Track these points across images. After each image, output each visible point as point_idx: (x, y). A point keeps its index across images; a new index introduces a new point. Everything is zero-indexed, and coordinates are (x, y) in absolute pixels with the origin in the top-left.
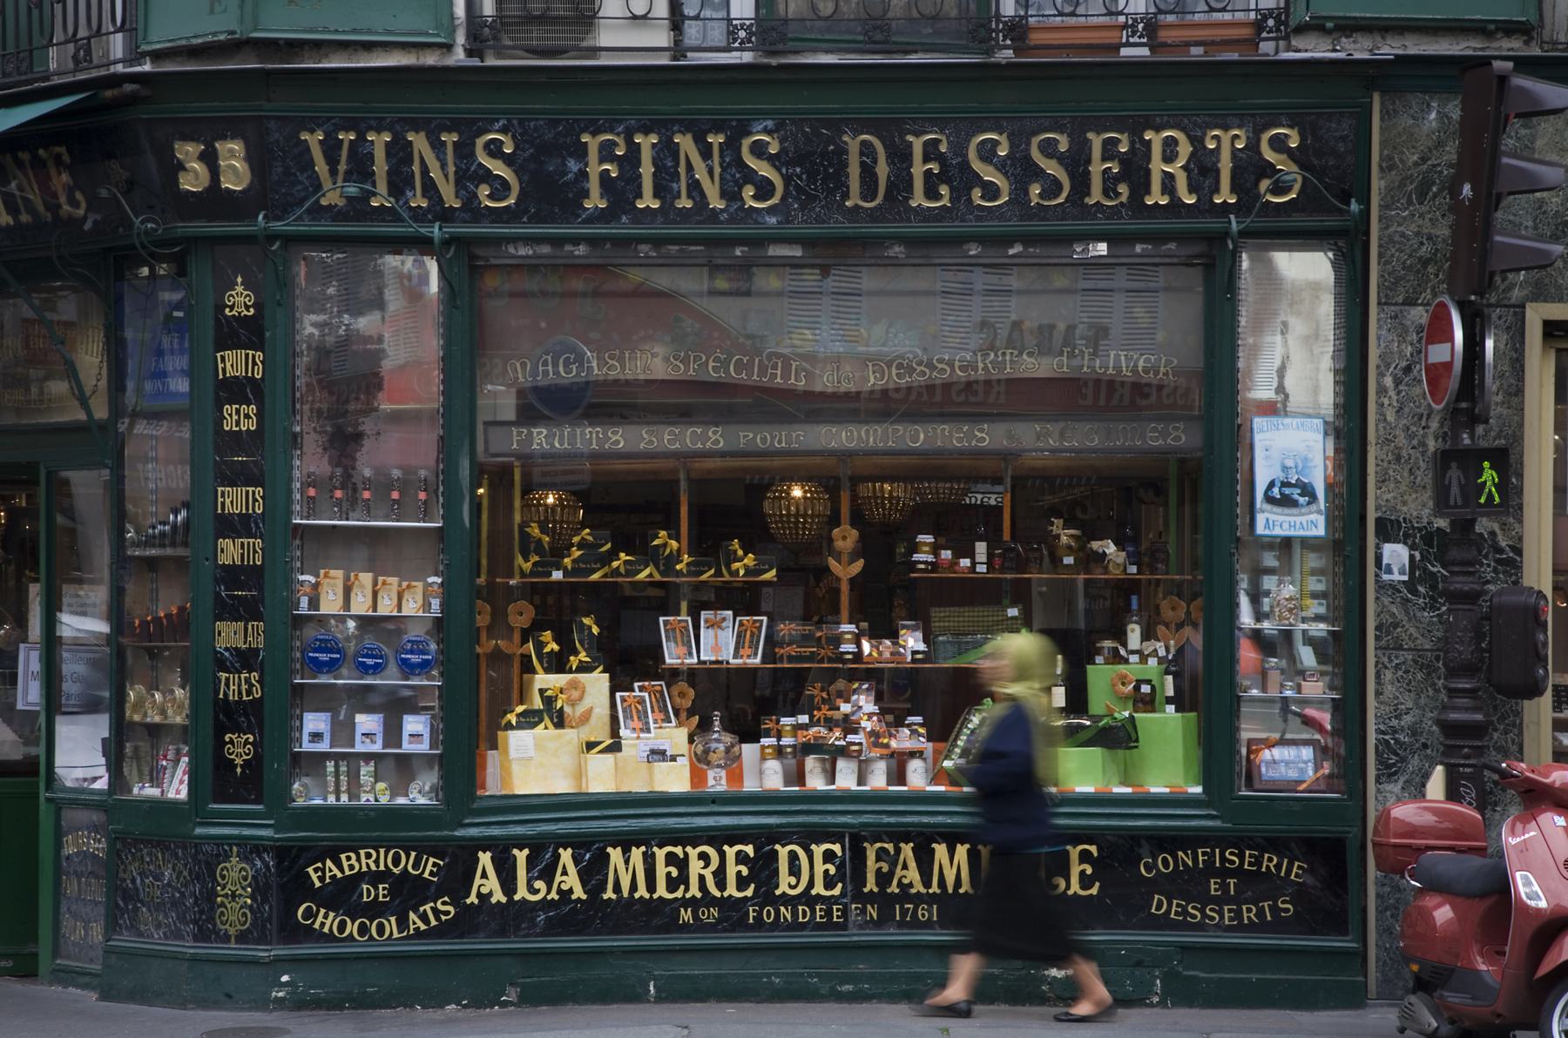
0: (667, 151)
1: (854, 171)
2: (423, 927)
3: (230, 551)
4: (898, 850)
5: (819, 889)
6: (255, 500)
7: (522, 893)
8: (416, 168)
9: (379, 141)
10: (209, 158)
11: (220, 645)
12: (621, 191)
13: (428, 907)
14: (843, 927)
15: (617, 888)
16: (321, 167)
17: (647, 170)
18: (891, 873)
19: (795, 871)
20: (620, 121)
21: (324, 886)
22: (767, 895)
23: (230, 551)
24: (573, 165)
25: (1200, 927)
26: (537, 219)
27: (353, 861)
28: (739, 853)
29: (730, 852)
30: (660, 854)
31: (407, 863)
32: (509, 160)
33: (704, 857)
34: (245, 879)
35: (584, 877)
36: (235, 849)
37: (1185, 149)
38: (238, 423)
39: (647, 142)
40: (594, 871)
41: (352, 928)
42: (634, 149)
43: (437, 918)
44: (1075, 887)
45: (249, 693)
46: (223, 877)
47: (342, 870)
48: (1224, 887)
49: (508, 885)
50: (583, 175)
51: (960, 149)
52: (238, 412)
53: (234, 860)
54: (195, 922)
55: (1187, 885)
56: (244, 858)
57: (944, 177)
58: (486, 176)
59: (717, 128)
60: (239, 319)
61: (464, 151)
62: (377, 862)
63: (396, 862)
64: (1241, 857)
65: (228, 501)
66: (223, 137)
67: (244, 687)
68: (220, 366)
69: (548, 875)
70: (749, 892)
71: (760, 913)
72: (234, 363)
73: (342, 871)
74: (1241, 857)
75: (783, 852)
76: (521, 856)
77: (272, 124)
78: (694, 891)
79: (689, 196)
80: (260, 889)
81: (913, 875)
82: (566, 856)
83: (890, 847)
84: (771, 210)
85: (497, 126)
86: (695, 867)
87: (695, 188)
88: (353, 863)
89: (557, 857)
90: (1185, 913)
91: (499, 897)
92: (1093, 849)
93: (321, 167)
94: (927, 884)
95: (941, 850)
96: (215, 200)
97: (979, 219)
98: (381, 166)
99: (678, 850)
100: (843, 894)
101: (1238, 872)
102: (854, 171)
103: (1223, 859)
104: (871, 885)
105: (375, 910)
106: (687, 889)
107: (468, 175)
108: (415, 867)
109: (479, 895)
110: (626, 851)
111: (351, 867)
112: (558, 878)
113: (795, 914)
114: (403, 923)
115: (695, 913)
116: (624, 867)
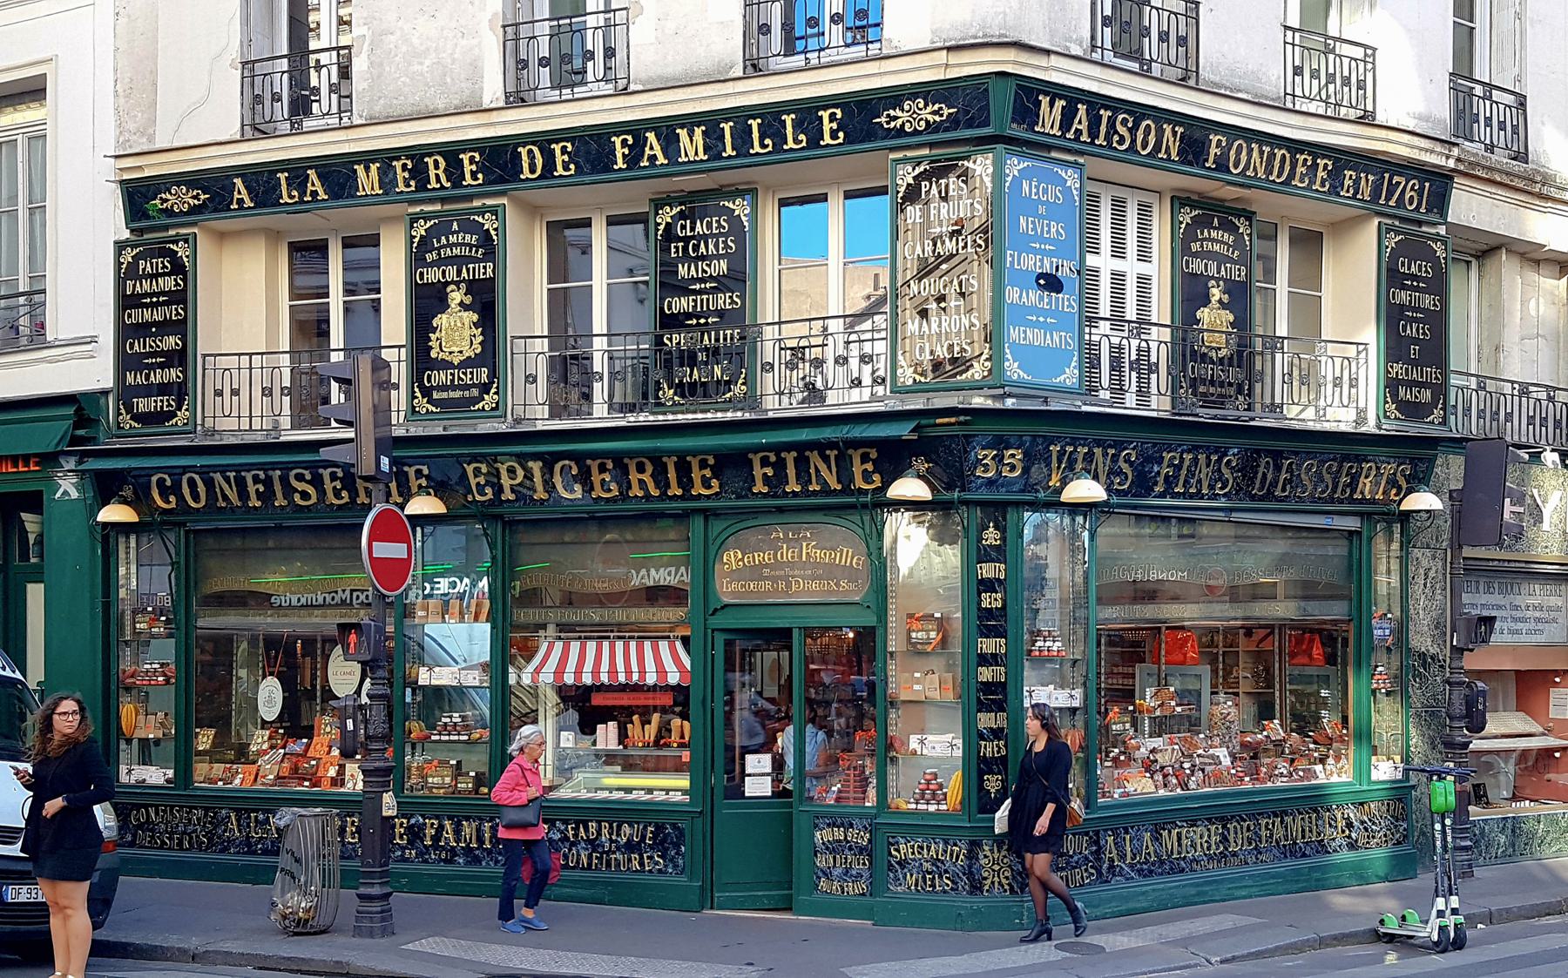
0: (1195, 461)
1: (1260, 475)
3: (986, 674)
6: (1000, 646)
8: (1093, 467)
11: (981, 726)
16: (1054, 464)
17: (1184, 472)
20: (1180, 445)
23: (986, 674)
24: (1156, 469)
32: (1131, 464)
37: (1373, 473)
38: (990, 603)
39: (1188, 457)
42: (1182, 460)
50: (1158, 473)
51: (1299, 466)
52: (990, 597)
57: (1290, 481)
58: (1120, 473)
60: (990, 546)
61: (1115, 458)
65: (984, 646)
67: (996, 749)
72: (987, 571)
84: (1224, 495)
85: (1132, 446)
87: (1199, 481)
93: (1054, 464)
102: (1260, 475)
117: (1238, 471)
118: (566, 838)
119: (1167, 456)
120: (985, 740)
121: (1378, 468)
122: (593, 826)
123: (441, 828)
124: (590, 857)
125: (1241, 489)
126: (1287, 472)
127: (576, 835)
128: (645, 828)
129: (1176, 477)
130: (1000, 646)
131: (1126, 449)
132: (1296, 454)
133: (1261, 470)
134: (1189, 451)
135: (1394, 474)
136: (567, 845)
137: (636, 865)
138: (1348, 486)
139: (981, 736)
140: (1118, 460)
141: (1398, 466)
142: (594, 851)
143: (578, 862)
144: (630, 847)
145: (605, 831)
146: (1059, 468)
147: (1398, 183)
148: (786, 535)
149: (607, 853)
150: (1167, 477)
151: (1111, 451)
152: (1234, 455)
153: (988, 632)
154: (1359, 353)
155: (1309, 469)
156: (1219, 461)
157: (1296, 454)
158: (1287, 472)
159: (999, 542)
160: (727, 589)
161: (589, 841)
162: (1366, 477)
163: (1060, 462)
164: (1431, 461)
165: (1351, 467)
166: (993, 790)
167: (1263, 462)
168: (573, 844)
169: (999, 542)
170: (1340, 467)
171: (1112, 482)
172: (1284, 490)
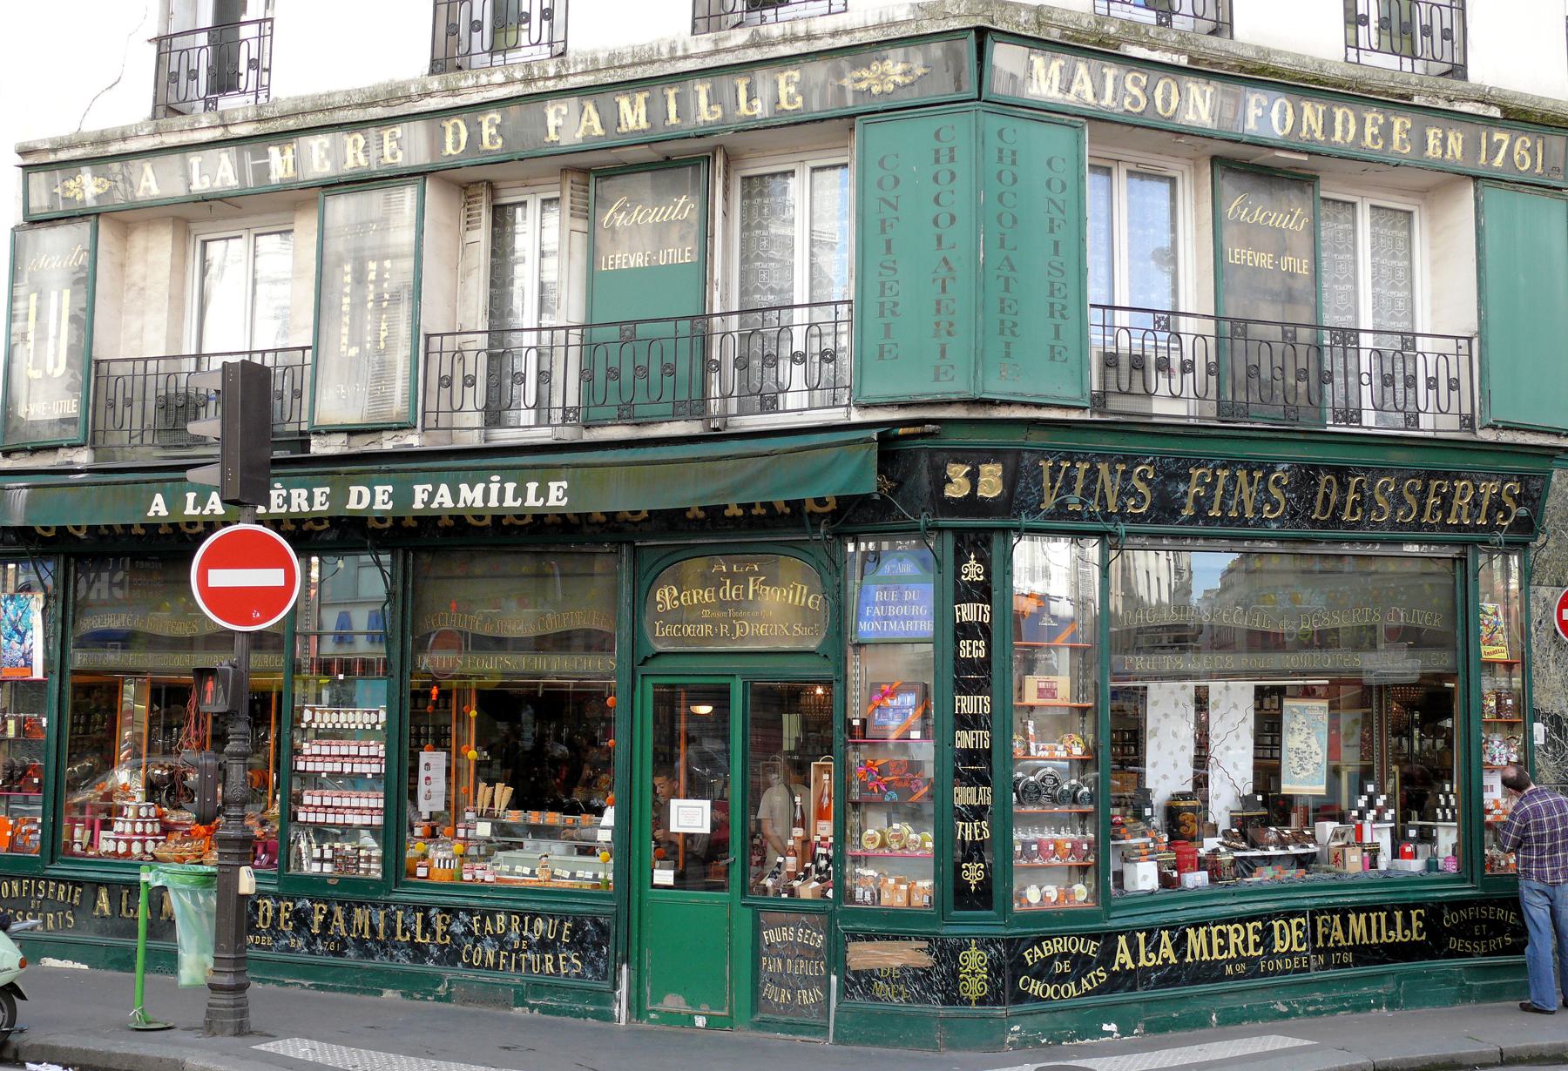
0: (1233, 478)
1: (1320, 497)
3: (965, 739)
4: (1332, 919)
5: (1295, 948)
6: (984, 705)
7: (1143, 962)
8: (1098, 486)
9: (1083, 467)
10: (973, 477)
11: (958, 803)
13: (1091, 975)
14: (1307, 970)
15: (1193, 955)
16: (1047, 484)
17: (1219, 492)
18: (1330, 934)
19: (1283, 938)
20: (1211, 461)
21: (1034, 964)
22: (1269, 954)
23: (965, 739)
24: (1182, 488)
25: (1470, 955)
26: (1156, 521)
29: (1250, 926)
30: (1214, 930)
31: (1079, 946)
32: (1149, 483)
33: (1237, 931)
34: (982, 961)
35: (1176, 947)
36: (973, 941)
37: (1471, 492)
38: (971, 653)
39: (1223, 474)
40: (1180, 944)
42: (1215, 477)
44: (1415, 937)
46: (965, 961)
48: (1481, 930)
49: (1135, 957)
50: (1186, 493)
51: (1372, 486)
52: (971, 645)
53: (973, 949)
54: (943, 992)
56: (980, 947)
57: (1361, 503)
58: (1134, 493)
59: (1260, 467)
60: (972, 583)
61: (1127, 475)
64: (1488, 911)
65: (963, 705)
66: (988, 462)
67: (977, 831)
68: (958, 614)
69: (1156, 949)
70: (1260, 952)
72: (968, 612)
74: (1488, 911)
75: (1276, 925)
76: (1141, 937)
77: (1026, 455)
78: (1233, 954)
80: (995, 968)
81: (1339, 934)
82: (1165, 934)
83: (1328, 918)
84: (1275, 520)
85: (1148, 461)
86: (1233, 937)
87: (1241, 503)
88: (1050, 948)
89: (1160, 936)
90: (1464, 947)
91: (1130, 965)
92: (1422, 911)
93: (1047, 484)
94: (1347, 941)
95: (1352, 917)
96: (972, 504)
97: (1372, 528)
99: (1223, 928)
100: (1307, 950)
101: (1487, 921)
102: (1320, 497)
103: (1480, 913)
104: (1320, 944)
105: (1062, 978)
108: (1084, 948)
109: (1120, 964)
110: (1197, 930)
111: (1049, 950)
112: (1162, 950)
114: (1078, 985)
115: (1234, 968)
116: (1196, 940)
117: (1290, 492)
118: (470, 933)
119: (1196, 473)
120: (962, 820)
121: (1476, 488)
122: (500, 918)
123: (330, 914)
124: (497, 955)
125: (1297, 513)
126: (1355, 492)
127: (481, 929)
128: (561, 923)
129: (1210, 498)
130: (984, 705)
131: (1141, 464)
132: (1366, 470)
133: (1321, 490)
134: (1224, 467)
135: (1499, 494)
136: (471, 940)
137: (549, 967)
138: (1438, 508)
142: (502, 948)
143: (483, 961)
144: (544, 945)
145: (515, 926)
146: (1052, 487)
147: (1501, 142)
148: (730, 568)
149: (517, 951)
150: (1197, 498)
151: (1121, 467)
152: (1284, 471)
153: (964, 688)
154: (1459, 347)
155: (1384, 489)
156: (1265, 478)
157: (1366, 470)
158: (1355, 492)
159: (982, 578)
160: (661, 636)
161: (495, 936)
162: (1462, 498)
163: (1053, 480)
165: (1440, 486)
168: (478, 940)
169: (982, 578)
170: (1426, 487)
171: (1125, 505)
172: (1353, 513)
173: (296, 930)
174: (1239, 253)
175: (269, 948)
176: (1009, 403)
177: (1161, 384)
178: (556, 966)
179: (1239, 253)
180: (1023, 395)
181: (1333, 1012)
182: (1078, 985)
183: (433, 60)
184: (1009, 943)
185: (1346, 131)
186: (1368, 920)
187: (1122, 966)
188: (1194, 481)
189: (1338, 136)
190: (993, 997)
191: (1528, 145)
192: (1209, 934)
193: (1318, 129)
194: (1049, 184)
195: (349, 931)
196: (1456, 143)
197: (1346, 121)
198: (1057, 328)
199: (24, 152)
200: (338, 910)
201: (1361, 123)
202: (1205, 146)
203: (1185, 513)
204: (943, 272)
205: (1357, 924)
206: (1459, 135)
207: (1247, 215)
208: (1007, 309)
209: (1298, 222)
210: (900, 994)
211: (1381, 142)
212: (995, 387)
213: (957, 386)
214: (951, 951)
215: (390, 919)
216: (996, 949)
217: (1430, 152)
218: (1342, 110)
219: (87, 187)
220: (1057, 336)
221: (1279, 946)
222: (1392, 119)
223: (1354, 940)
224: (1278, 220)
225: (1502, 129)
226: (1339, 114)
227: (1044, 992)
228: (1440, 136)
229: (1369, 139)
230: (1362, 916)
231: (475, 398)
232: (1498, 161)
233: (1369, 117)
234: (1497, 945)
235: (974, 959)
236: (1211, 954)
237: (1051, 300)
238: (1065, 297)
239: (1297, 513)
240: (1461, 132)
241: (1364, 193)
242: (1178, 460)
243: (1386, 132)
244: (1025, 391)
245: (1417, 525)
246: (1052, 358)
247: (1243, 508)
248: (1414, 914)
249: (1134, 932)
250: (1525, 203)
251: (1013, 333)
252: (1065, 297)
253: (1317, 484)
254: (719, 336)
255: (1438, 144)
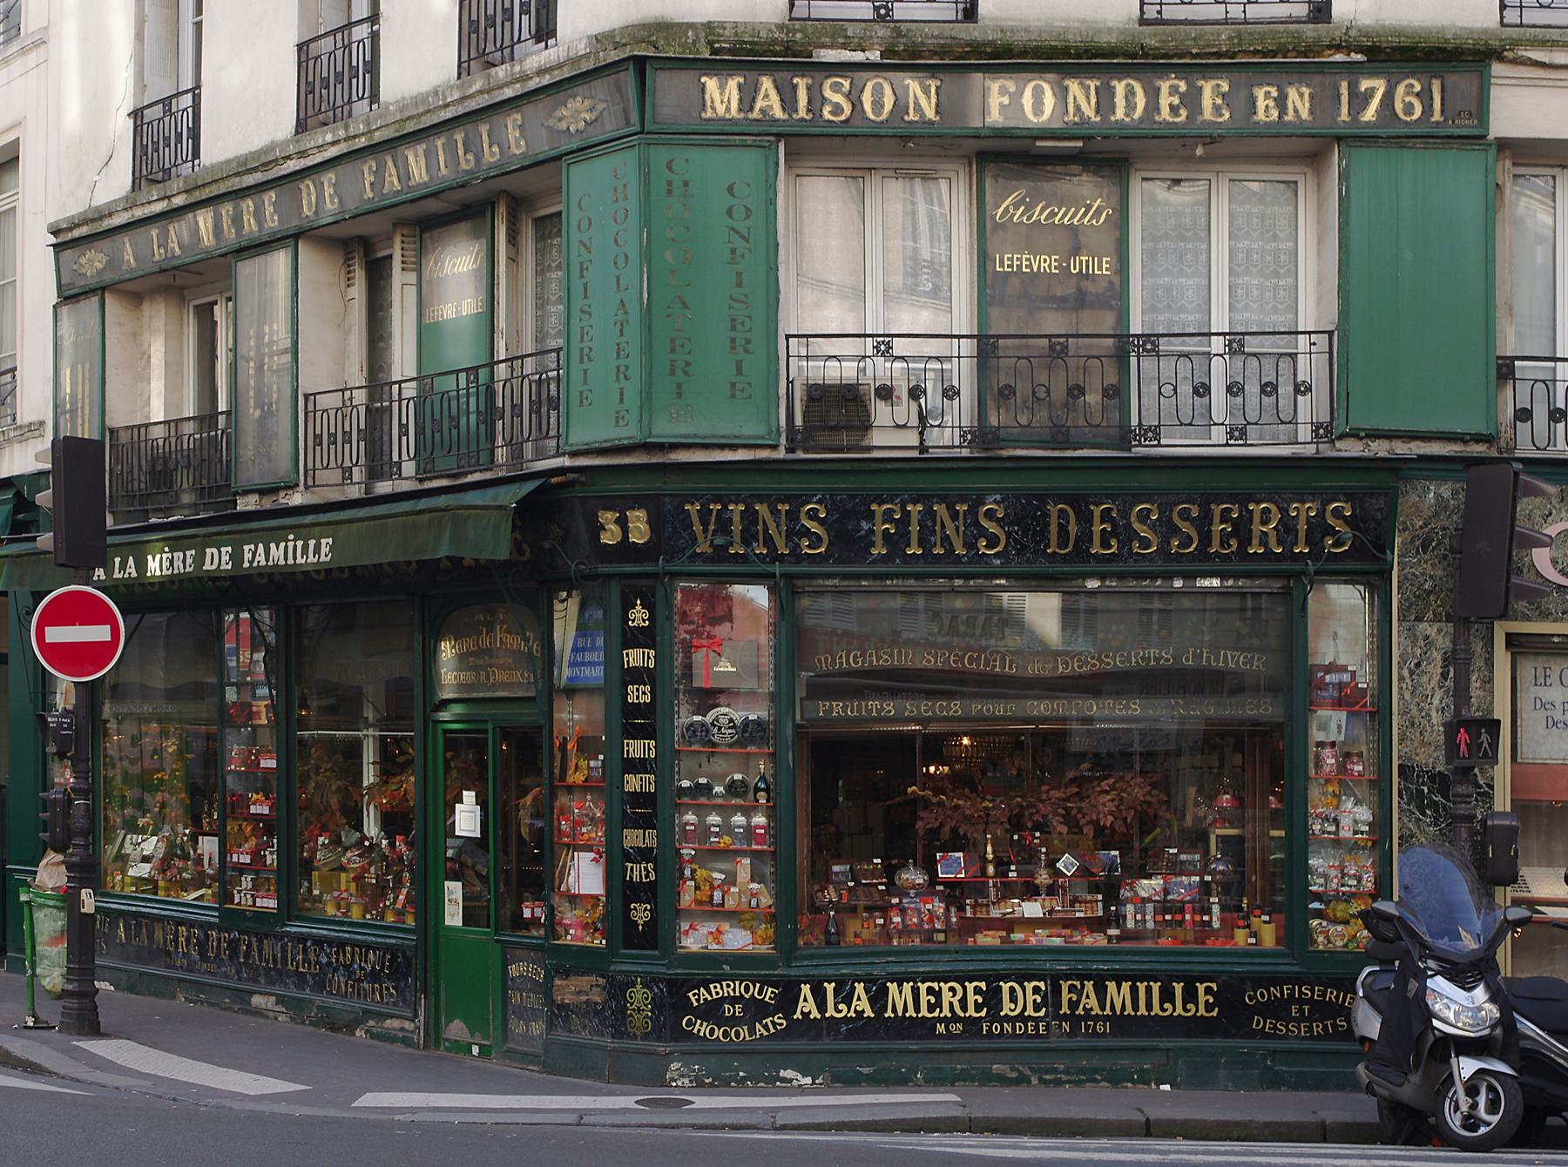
0: (929, 514)
1: (1054, 528)
2: (766, 1033)
3: (633, 783)
4: (1083, 986)
5: (1030, 1012)
7: (830, 1012)
12: (895, 542)
13: (768, 1020)
15: (894, 1010)
17: (914, 528)
18: (1079, 1001)
19: (1013, 999)
20: (897, 496)
21: (700, 1005)
22: (994, 1016)
23: (633, 783)
24: (865, 525)
25: (1285, 1037)
26: (839, 561)
27: (718, 989)
28: (976, 987)
29: (970, 987)
30: (923, 987)
31: (754, 991)
32: (822, 522)
33: (952, 989)
35: (872, 1001)
38: (638, 698)
39: (915, 509)
40: (878, 998)
41: (719, 1033)
42: (906, 515)
43: (775, 1028)
44: (1202, 1011)
45: (647, 877)
47: (711, 995)
48: (1301, 1011)
50: (871, 531)
51: (1125, 514)
53: (639, 986)
54: (613, 1026)
55: (1276, 1009)
56: (645, 985)
57: (1114, 533)
58: (806, 532)
59: (963, 500)
61: (793, 516)
62: (734, 990)
63: (747, 989)
67: (644, 873)
70: (983, 1014)
71: (991, 1027)
72: (635, 657)
73: (711, 995)
75: (1005, 987)
76: (830, 988)
78: (946, 1012)
79: (942, 545)
80: (657, 1005)
81: (1093, 1002)
82: (860, 987)
83: (1078, 984)
85: (815, 499)
86: (947, 996)
87: (946, 540)
88: (718, 990)
90: (1275, 1028)
91: (815, 1014)
94: (1103, 1009)
95: (1112, 986)
97: (1136, 561)
98: (737, 527)
99: (935, 985)
100: (1046, 1015)
101: (1311, 1001)
102: (1054, 528)
104: (1065, 1009)
105: (733, 1021)
106: (941, 1012)
107: (795, 532)
109: (802, 1012)
110: (900, 985)
111: (717, 993)
112: (855, 1002)
113: (1014, 1028)
114: (752, 1031)
115: (947, 1028)
116: (899, 997)
125: (1024, 547)
131: (809, 503)
132: (1113, 497)
139: (627, 856)
140: (798, 518)
141: (1325, 504)
151: (785, 507)
163: (705, 525)
164: (1393, 496)
166: (641, 922)
167: (1054, 510)
173: (231, 958)
174: (1011, 259)
175: (214, 974)
176: (688, 446)
177: (881, 413)
178: (381, 996)
179: (1011, 259)
180: (696, 436)
181: (1079, 1083)
182: (752, 1031)
183: (298, 120)
184: (672, 983)
185: (1130, 106)
186: (1134, 991)
187: (806, 1015)
188: (879, 518)
189: (1120, 113)
190: (657, 1034)
191: (1418, 88)
192: (916, 992)
193: (1089, 111)
194: (729, 212)
195: (261, 961)
196: (1299, 101)
197: (1130, 93)
198: (739, 363)
199: (56, 232)
200: (254, 940)
201: (1153, 95)
202: (960, 145)
203: (875, 552)
204: (621, 317)
205: (1118, 995)
206: (1306, 91)
207: (1022, 215)
208: (678, 349)
209: (1098, 213)
210: (584, 1028)
211: (1184, 113)
212: (664, 430)
213: (628, 432)
214: (621, 990)
215: (284, 950)
216: (659, 988)
217: (1261, 116)
218: (1124, 83)
219: (92, 262)
220: (739, 372)
221: (1007, 1008)
222: (1201, 83)
223: (1113, 1008)
224: (1063, 216)
225: (1373, 74)
226: (1120, 88)
227: (712, 1032)
228: (1275, 94)
229: (1165, 113)
230: (1126, 986)
231: (357, 450)
232: (1370, 114)
233: (1165, 86)
234: (1325, 1028)
235: (639, 996)
236: (917, 1010)
237: (733, 334)
238: (750, 330)
239: (1024, 547)
240: (1308, 86)
241: (1219, 167)
242: (853, 497)
243: (1191, 100)
244: (738, 432)
245: (1203, 554)
246: (733, 396)
247: (951, 544)
248: (1201, 988)
249: (821, 983)
250: (1409, 162)
251: (686, 373)
252: (750, 330)
253: (1046, 515)
254: (502, 383)
255: (1271, 103)
